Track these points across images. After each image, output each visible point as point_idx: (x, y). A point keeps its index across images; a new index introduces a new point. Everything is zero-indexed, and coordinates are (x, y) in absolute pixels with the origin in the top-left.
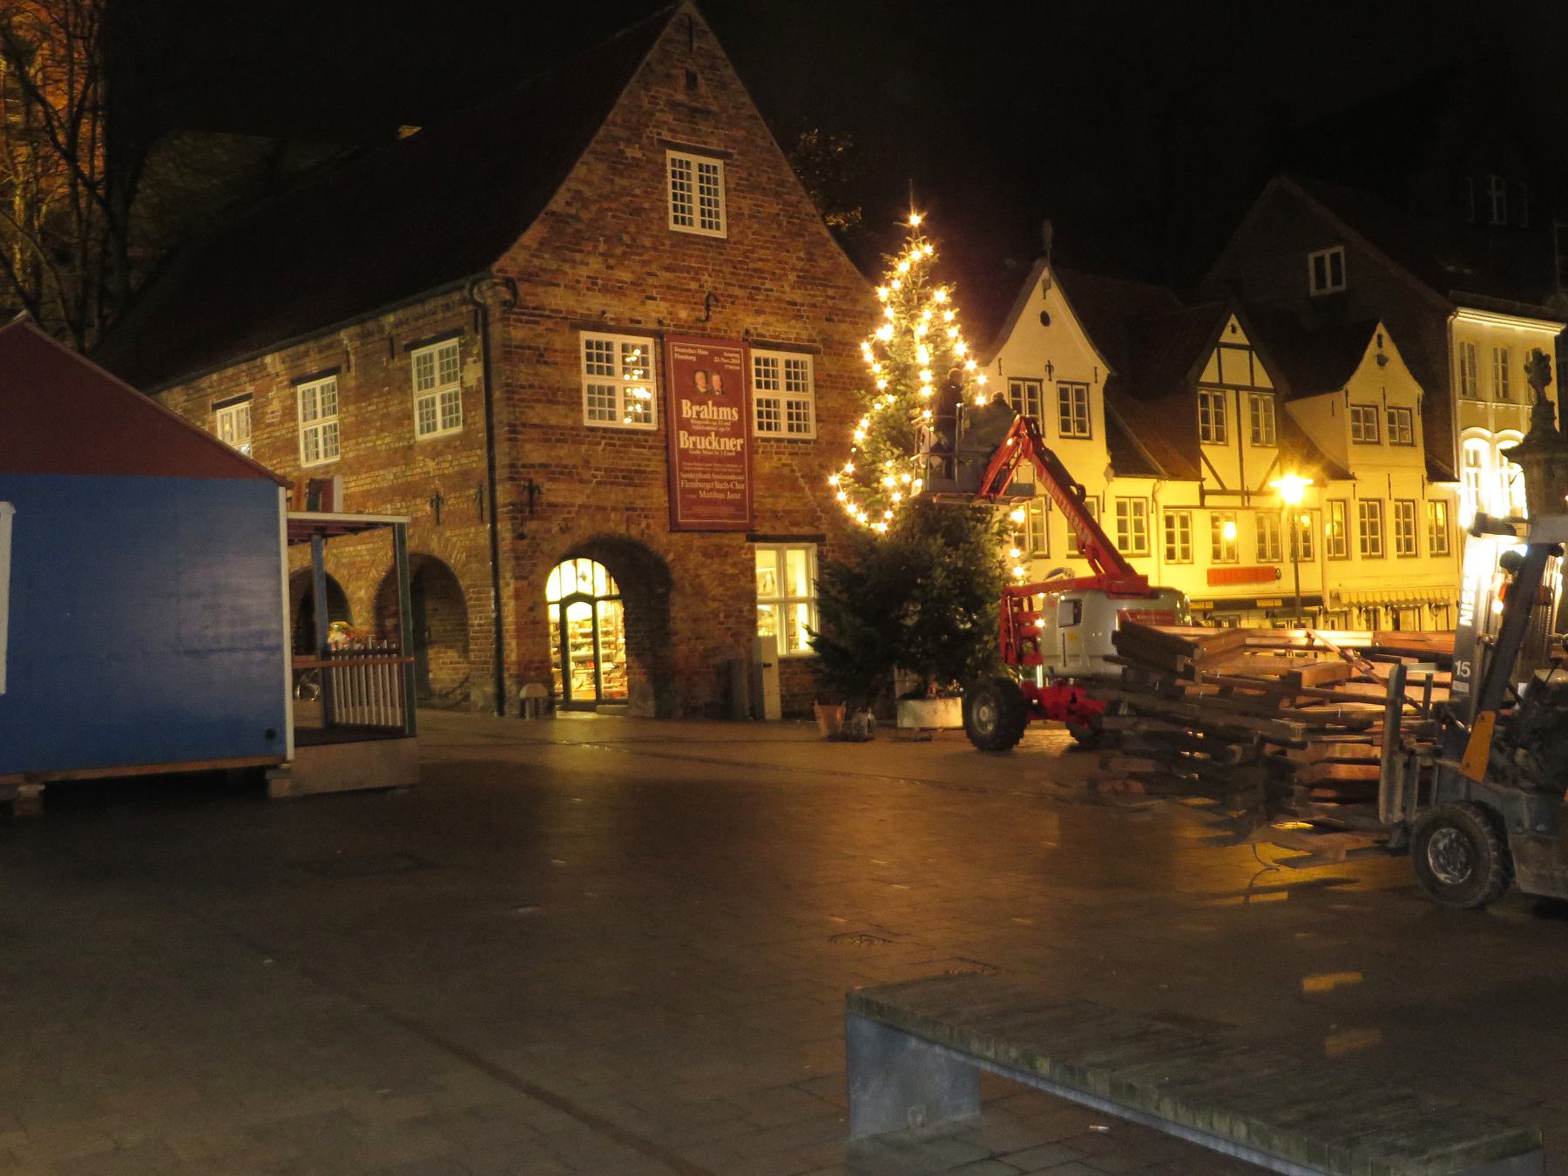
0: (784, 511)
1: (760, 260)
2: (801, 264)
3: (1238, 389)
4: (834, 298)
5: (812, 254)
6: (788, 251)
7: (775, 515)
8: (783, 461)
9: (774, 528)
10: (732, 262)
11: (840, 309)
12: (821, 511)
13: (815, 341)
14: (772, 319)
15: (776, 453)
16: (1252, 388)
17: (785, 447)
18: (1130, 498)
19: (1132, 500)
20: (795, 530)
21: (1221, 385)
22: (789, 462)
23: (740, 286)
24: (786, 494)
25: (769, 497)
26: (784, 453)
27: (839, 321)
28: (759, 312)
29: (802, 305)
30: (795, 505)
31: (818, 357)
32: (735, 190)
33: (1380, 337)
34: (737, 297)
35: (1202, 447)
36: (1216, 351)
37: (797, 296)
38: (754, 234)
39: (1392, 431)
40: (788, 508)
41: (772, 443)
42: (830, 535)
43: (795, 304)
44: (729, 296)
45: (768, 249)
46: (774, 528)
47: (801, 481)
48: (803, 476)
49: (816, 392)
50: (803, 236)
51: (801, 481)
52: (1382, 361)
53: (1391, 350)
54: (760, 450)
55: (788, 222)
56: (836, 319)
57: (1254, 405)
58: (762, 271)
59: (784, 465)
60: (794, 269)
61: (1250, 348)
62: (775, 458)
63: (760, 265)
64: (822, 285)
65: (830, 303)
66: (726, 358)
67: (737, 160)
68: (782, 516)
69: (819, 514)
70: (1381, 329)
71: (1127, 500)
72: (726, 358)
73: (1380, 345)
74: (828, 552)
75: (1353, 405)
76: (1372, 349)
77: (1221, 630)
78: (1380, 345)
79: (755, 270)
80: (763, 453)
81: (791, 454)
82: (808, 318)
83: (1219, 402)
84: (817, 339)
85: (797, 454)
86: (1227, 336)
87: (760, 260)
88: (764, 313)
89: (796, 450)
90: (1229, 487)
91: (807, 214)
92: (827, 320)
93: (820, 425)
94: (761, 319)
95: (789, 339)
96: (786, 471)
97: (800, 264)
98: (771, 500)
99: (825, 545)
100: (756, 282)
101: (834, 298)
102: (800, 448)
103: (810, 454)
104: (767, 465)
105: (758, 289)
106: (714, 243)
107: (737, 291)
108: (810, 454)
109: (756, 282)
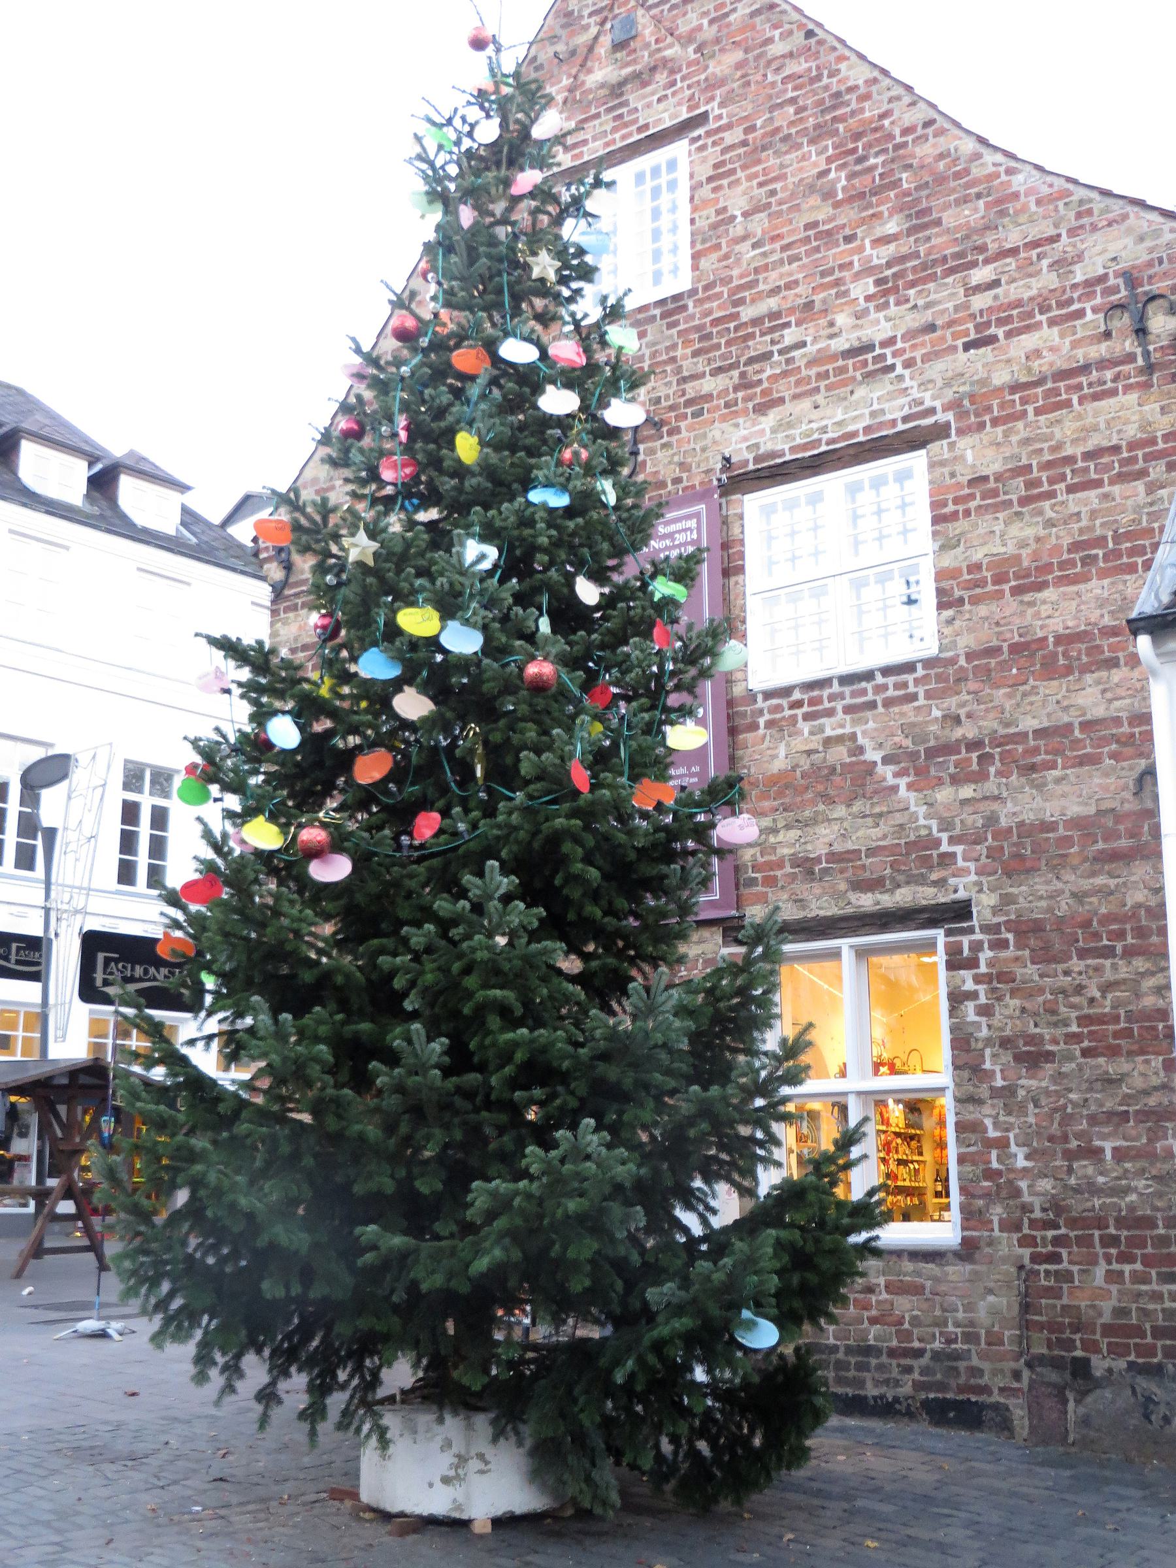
0: (833, 857)
1: (775, 291)
2: (890, 250)
4: (996, 283)
5: (927, 211)
6: (849, 239)
7: (806, 867)
8: (829, 732)
9: (800, 902)
10: (699, 328)
11: (1018, 304)
12: (952, 840)
13: (932, 411)
14: (806, 404)
15: (807, 717)
17: (832, 698)
20: (866, 902)
22: (848, 730)
23: (719, 370)
24: (840, 811)
25: (788, 827)
26: (830, 713)
27: (1009, 335)
28: (761, 409)
29: (891, 341)
30: (866, 835)
31: (939, 448)
32: (710, 179)
34: (708, 397)
37: (878, 328)
38: (755, 246)
40: (838, 848)
41: (836, 687)
42: (984, 905)
43: (870, 347)
44: (689, 403)
45: (792, 259)
46: (800, 902)
47: (887, 772)
48: (886, 760)
49: (935, 534)
50: (897, 183)
51: (887, 772)
54: (762, 721)
55: (851, 176)
56: (1000, 333)
58: (774, 315)
59: (828, 742)
60: (868, 270)
62: (805, 727)
63: (773, 303)
64: (952, 271)
65: (980, 302)
66: (665, 537)
67: (720, 117)
68: (825, 871)
69: (945, 847)
72: (665, 537)
74: (976, 947)
77: (1016, 1385)
79: (756, 322)
80: (770, 724)
81: (848, 710)
82: (908, 364)
84: (938, 404)
85: (872, 705)
87: (775, 291)
88: (781, 401)
89: (870, 697)
91: (906, 131)
92: (967, 347)
93: (949, 613)
94: (769, 421)
95: (854, 434)
96: (839, 754)
97: (880, 256)
98: (793, 834)
99: (971, 930)
100: (759, 345)
101: (996, 283)
102: (885, 687)
103: (913, 697)
104: (782, 751)
105: (767, 356)
106: (657, 312)
107: (709, 385)
108: (913, 697)
109: (759, 345)
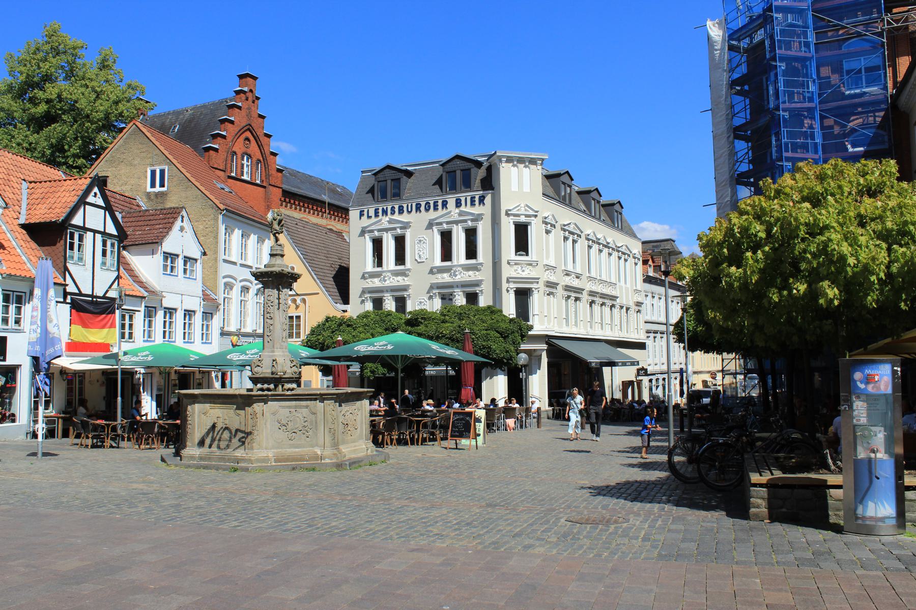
3: (95, 232)
16: (104, 233)
18: (13, 291)
19: (15, 293)
21: (85, 229)
33: (183, 217)
35: (68, 265)
36: (82, 209)
39: (185, 271)
52: (182, 229)
53: (186, 224)
57: (104, 244)
61: (105, 209)
70: (184, 213)
71: (11, 293)
73: (182, 221)
75: (164, 253)
76: (178, 224)
78: (182, 221)
83: (81, 238)
86: (90, 199)
90: (83, 292)
